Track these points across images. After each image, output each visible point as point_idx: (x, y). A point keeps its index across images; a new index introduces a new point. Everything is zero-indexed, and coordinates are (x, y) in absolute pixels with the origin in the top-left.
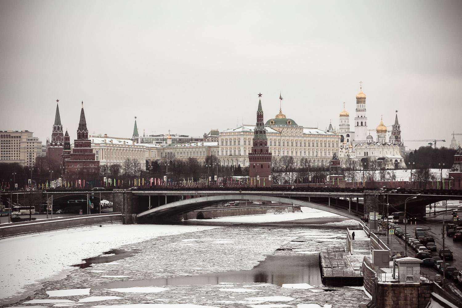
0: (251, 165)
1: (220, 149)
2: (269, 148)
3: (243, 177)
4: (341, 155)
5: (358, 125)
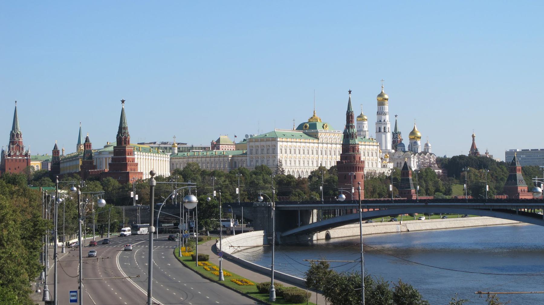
1: (248, 158)
3: (353, 189)
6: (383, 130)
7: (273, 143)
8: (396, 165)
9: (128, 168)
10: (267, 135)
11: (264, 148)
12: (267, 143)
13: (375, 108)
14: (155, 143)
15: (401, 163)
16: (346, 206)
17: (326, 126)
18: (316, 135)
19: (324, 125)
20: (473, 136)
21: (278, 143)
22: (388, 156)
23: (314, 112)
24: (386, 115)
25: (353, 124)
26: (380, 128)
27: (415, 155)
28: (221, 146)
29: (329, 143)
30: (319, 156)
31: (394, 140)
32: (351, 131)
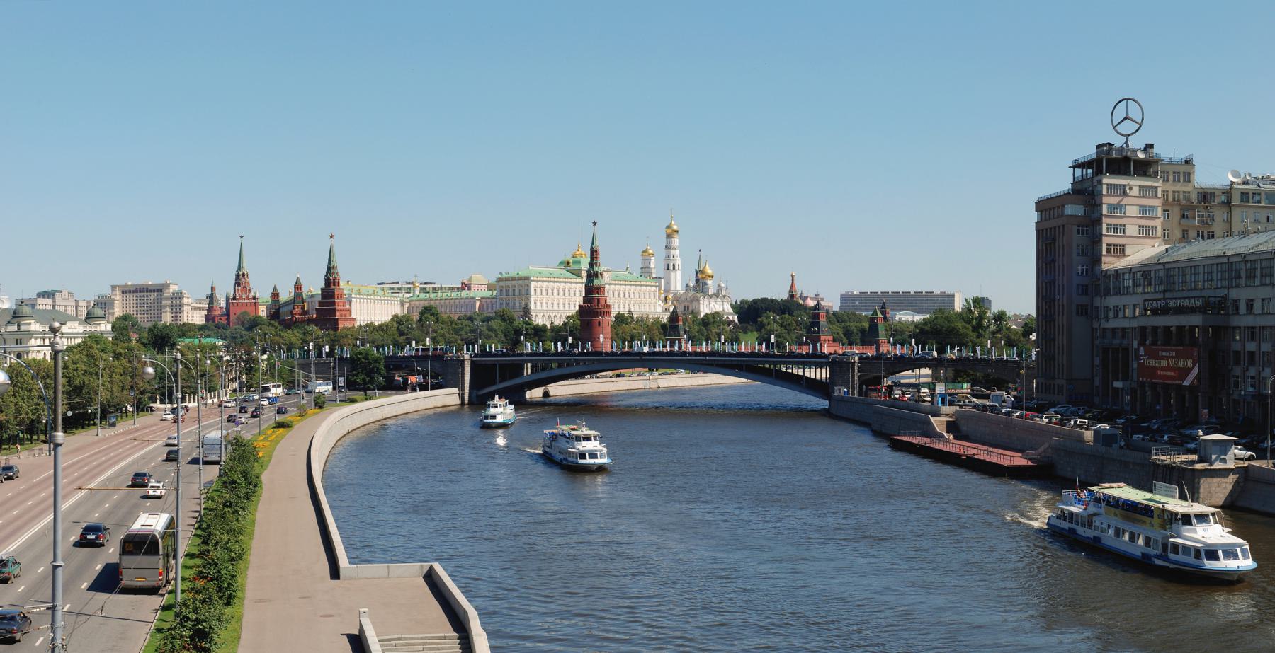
6: (671, 267)
9: (338, 314)
13: (664, 241)
14: (398, 283)
15: (688, 307)
16: (578, 360)
20: (792, 276)
28: (472, 286)
32: (596, 269)
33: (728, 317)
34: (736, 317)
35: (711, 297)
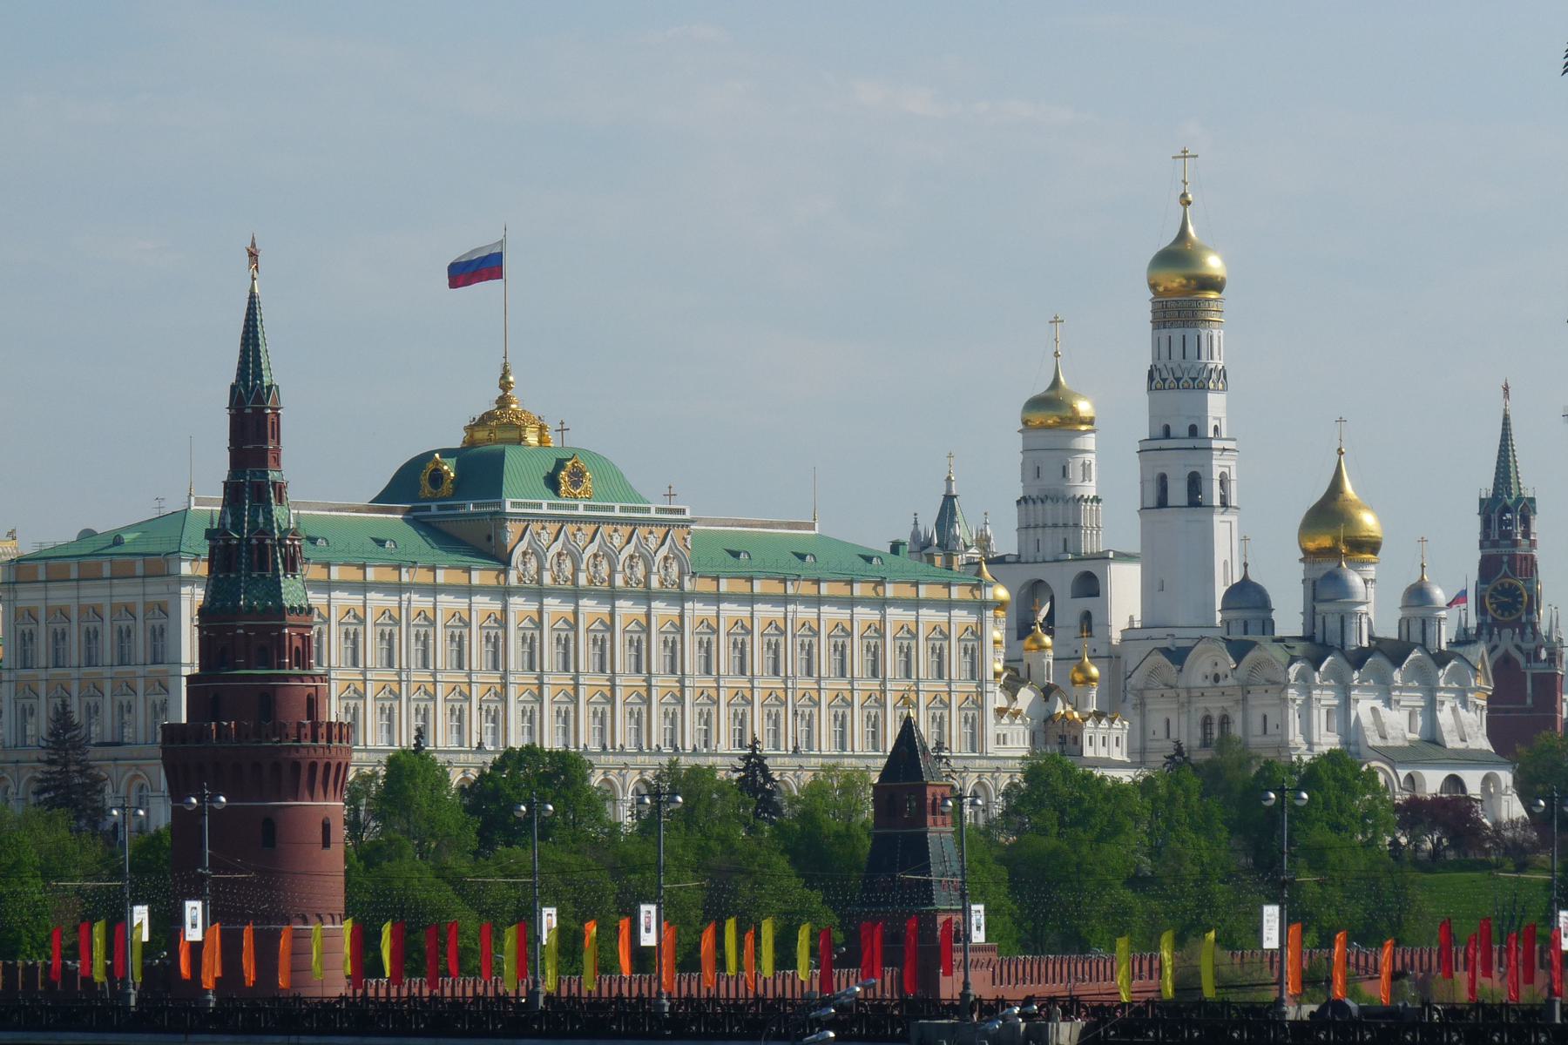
0: (183, 821)
2: (335, 689)
4: (1001, 739)
5: (1162, 503)
6: (1178, 492)
7: (155, 590)
8: (1198, 732)
10: (127, 537)
11: (98, 624)
12: (83, 592)
15: (1225, 721)
17: (577, 477)
18: (489, 538)
19: (560, 464)
21: (185, 590)
22: (1094, 671)
23: (504, 376)
24: (1204, 388)
25: (273, 475)
26: (1163, 480)
27: (1317, 668)
29: (659, 596)
30: (511, 679)
31: (1493, 551)
33: (1455, 782)
34: (1506, 777)
35: (1358, 659)
